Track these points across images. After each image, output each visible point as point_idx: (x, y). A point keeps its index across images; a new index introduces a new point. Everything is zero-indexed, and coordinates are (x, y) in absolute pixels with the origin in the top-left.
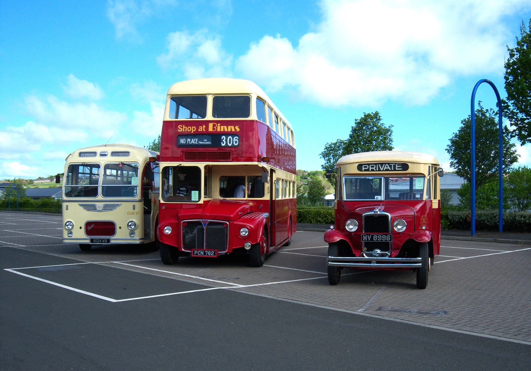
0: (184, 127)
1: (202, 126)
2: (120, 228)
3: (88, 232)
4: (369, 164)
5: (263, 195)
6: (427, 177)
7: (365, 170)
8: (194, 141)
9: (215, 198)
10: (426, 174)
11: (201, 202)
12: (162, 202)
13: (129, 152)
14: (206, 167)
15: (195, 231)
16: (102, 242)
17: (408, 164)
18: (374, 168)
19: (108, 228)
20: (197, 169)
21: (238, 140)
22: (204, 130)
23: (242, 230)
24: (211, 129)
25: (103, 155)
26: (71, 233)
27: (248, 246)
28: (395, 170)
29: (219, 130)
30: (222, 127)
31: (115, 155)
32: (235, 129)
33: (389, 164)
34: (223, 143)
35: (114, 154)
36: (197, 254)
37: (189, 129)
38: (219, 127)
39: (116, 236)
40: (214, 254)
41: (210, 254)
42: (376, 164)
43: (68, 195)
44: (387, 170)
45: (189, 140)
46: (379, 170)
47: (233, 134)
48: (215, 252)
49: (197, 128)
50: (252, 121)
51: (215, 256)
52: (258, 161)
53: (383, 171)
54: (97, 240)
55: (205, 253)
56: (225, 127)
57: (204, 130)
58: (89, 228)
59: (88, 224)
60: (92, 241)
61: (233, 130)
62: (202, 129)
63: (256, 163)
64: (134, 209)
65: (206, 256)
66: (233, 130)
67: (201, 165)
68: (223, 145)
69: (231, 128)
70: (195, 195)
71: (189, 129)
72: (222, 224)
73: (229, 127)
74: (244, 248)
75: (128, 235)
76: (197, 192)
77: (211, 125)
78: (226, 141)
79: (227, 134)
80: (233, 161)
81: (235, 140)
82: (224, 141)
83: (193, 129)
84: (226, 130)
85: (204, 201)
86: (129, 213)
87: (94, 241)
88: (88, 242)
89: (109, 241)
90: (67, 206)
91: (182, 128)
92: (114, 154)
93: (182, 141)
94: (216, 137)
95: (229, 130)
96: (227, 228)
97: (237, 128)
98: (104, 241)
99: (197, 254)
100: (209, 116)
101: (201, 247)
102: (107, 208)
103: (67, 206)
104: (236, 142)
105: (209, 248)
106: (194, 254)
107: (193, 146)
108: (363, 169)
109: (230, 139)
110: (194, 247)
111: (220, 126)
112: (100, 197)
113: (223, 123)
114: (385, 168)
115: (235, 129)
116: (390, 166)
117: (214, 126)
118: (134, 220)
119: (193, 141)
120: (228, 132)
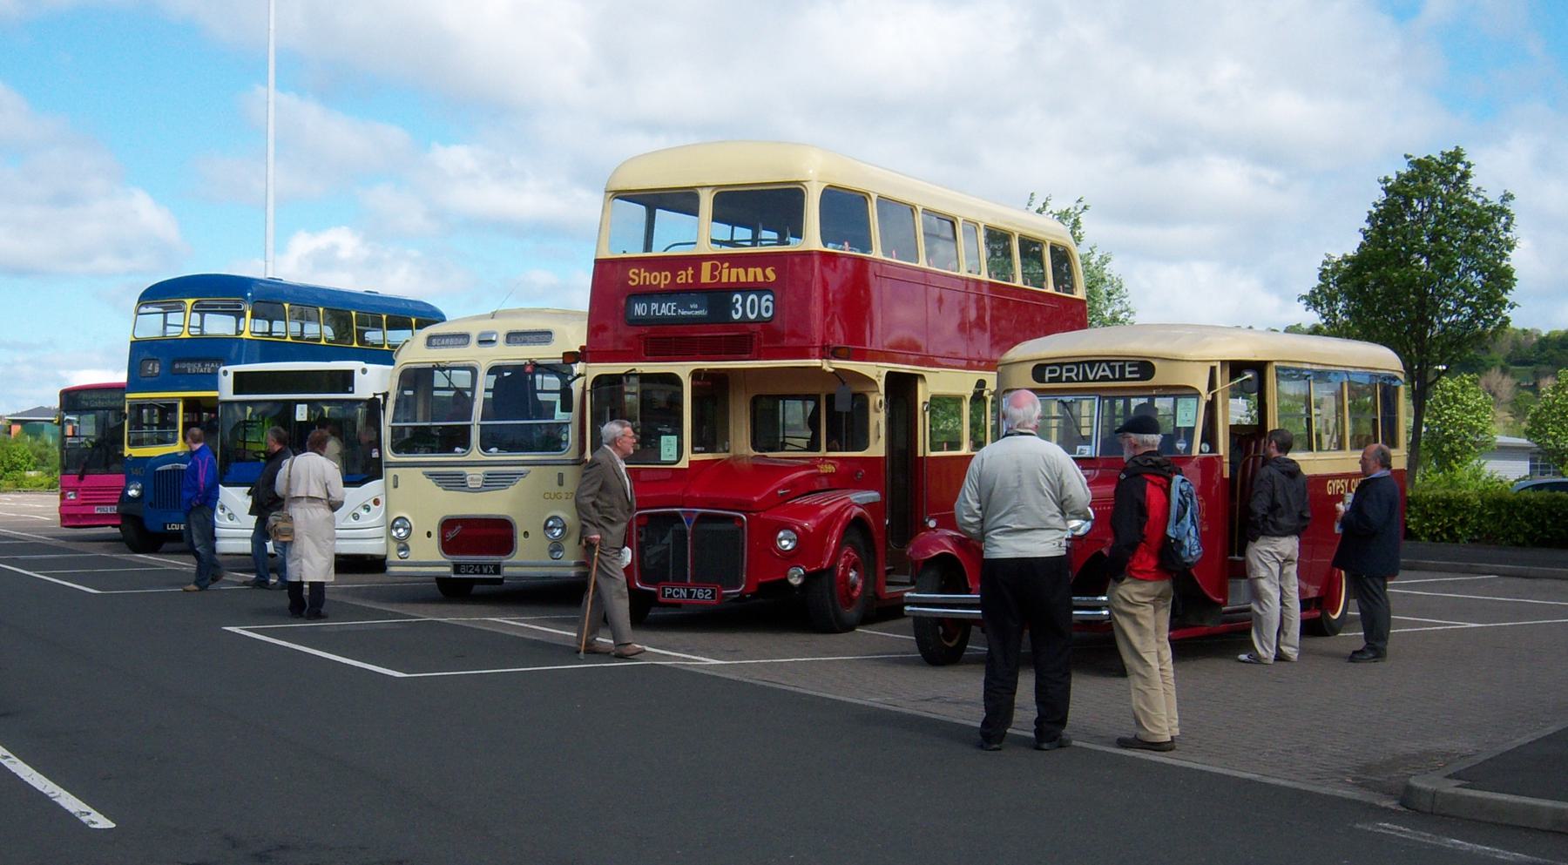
2: (526, 534)
3: (448, 547)
4: (1061, 365)
6: (1206, 396)
7: (1052, 380)
9: (738, 453)
10: (1202, 386)
11: (684, 464)
13: (549, 333)
14: (696, 375)
15: (669, 539)
17: (1155, 363)
18: (1073, 375)
19: (493, 535)
20: (673, 380)
23: (781, 534)
24: (705, 278)
25: (485, 341)
26: (406, 548)
28: (1122, 378)
29: (725, 280)
30: (734, 271)
31: (516, 342)
32: (765, 276)
33: (1108, 362)
35: (514, 337)
38: (725, 272)
39: (518, 556)
41: (703, 595)
42: (1077, 364)
43: (396, 449)
44: (1104, 379)
45: (655, 306)
46: (1086, 379)
47: (759, 288)
49: (674, 276)
50: (808, 255)
52: (822, 357)
53: (1094, 380)
54: (468, 566)
55: (690, 594)
56: (741, 271)
58: (450, 535)
59: (448, 524)
61: (760, 278)
62: (685, 277)
63: (816, 362)
64: (561, 484)
67: (683, 370)
68: (736, 317)
69: (755, 274)
70: (668, 446)
73: (751, 270)
74: (785, 582)
75: (547, 553)
76: (675, 438)
77: (706, 267)
78: (744, 305)
79: (745, 289)
81: (764, 304)
82: (738, 306)
83: (662, 279)
84: (743, 279)
86: (548, 496)
88: (447, 570)
89: (497, 568)
90: (396, 477)
92: (514, 337)
93: (639, 309)
94: (719, 296)
95: (751, 279)
97: (769, 271)
99: (670, 596)
101: (680, 580)
102: (493, 482)
103: (396, 477)
104: (767, 309)
105: (700, 581)
107: (665, 321)
108: (1047, 376)
110: (666, 579)
112: (476, 453)
114: (1100, 373)
115: (765, 276)
116: (1112, 369)
117: (714, 268)
118: (561, 515)
119: (665, 310)
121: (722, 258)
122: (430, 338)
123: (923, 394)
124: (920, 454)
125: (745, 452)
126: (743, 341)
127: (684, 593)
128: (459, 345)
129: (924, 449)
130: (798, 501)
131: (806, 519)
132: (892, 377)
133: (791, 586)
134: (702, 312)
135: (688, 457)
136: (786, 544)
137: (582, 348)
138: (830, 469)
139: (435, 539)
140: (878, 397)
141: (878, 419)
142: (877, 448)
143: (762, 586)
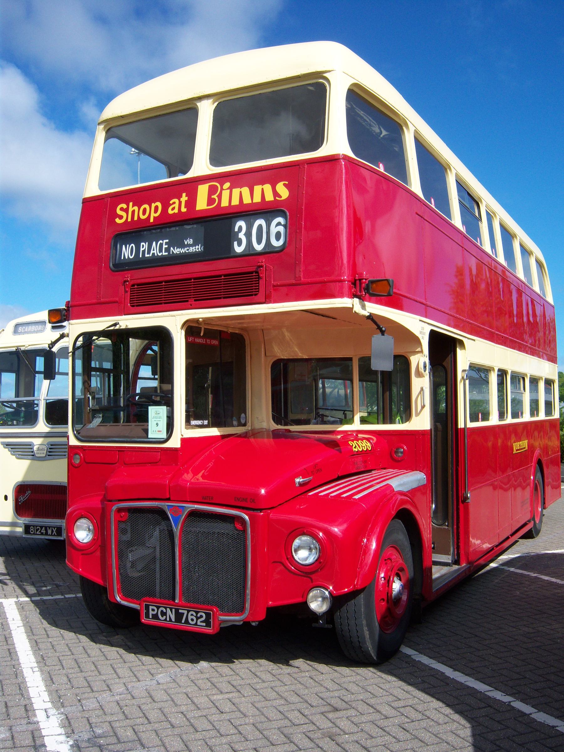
1: (179, 197)
3: (19, 509)
5: (407, 416)
8: (157, 249)
9: (257, 426)
11: (175, 443)
12: (73, 442)
14: (191, 329)
16: (46, 534)
20: (160, 336)
21: (285, 226)
22: (184, 210)
23: (297, 542)
24: (202, 204)
30: (236, 192)
34: (240, 244)
37: (145, 210)
38: (225, 195)
40: (207, 622)
41: (195, 621)
47: (267, 210)
48: (208, 615)
49: (166, 206)
51: (209, 630)
55: (179, 616)
58: (22, 499)
60: (27, 528)
61: (269, 197)
62: (177, 206)
65: (182, 626)
66: (269, 197)
67: (174, 321)
69: (264, 192)
73: (258, 189)
74: (305, 605)
76: (163, 410)
77: (203, 190)
78: (248, 235)
80: (267, 300)
81: (274, 230)
82: (242, 236)
83: (151, 212)
84: (247, 200)
87: (32, 529)
91: (126, 211)
93: (127, 252)
94: (218, 224)
95: (257, 199)
96: (245, 530)
98: (50, 532)
99: (155, 617)
100: (201, 165)
106: (147, 615)
107: (156, 262)
109: (260, 227)
111: (231, 188)
117: (213, 190)
119: (155, 251)
120: (253, 204)
121: (221, 178)
122: (17, 326)
123: (464, 359)
124: (461, 425)
125: (264, 425)
126: (245, 282)
128: (37, 332)
129: (464, 421)
130: (323, 491)
131: (333, 522)
132: (434, 336)
134: (198, 248)
135: (182, 431)
136: (304, 554)
137: (68, 303)
138: (364, 446)
139: (10, 503)
140: (420, 360)
141: (421, 385)
142: (421, 421)
143: (271, 611)
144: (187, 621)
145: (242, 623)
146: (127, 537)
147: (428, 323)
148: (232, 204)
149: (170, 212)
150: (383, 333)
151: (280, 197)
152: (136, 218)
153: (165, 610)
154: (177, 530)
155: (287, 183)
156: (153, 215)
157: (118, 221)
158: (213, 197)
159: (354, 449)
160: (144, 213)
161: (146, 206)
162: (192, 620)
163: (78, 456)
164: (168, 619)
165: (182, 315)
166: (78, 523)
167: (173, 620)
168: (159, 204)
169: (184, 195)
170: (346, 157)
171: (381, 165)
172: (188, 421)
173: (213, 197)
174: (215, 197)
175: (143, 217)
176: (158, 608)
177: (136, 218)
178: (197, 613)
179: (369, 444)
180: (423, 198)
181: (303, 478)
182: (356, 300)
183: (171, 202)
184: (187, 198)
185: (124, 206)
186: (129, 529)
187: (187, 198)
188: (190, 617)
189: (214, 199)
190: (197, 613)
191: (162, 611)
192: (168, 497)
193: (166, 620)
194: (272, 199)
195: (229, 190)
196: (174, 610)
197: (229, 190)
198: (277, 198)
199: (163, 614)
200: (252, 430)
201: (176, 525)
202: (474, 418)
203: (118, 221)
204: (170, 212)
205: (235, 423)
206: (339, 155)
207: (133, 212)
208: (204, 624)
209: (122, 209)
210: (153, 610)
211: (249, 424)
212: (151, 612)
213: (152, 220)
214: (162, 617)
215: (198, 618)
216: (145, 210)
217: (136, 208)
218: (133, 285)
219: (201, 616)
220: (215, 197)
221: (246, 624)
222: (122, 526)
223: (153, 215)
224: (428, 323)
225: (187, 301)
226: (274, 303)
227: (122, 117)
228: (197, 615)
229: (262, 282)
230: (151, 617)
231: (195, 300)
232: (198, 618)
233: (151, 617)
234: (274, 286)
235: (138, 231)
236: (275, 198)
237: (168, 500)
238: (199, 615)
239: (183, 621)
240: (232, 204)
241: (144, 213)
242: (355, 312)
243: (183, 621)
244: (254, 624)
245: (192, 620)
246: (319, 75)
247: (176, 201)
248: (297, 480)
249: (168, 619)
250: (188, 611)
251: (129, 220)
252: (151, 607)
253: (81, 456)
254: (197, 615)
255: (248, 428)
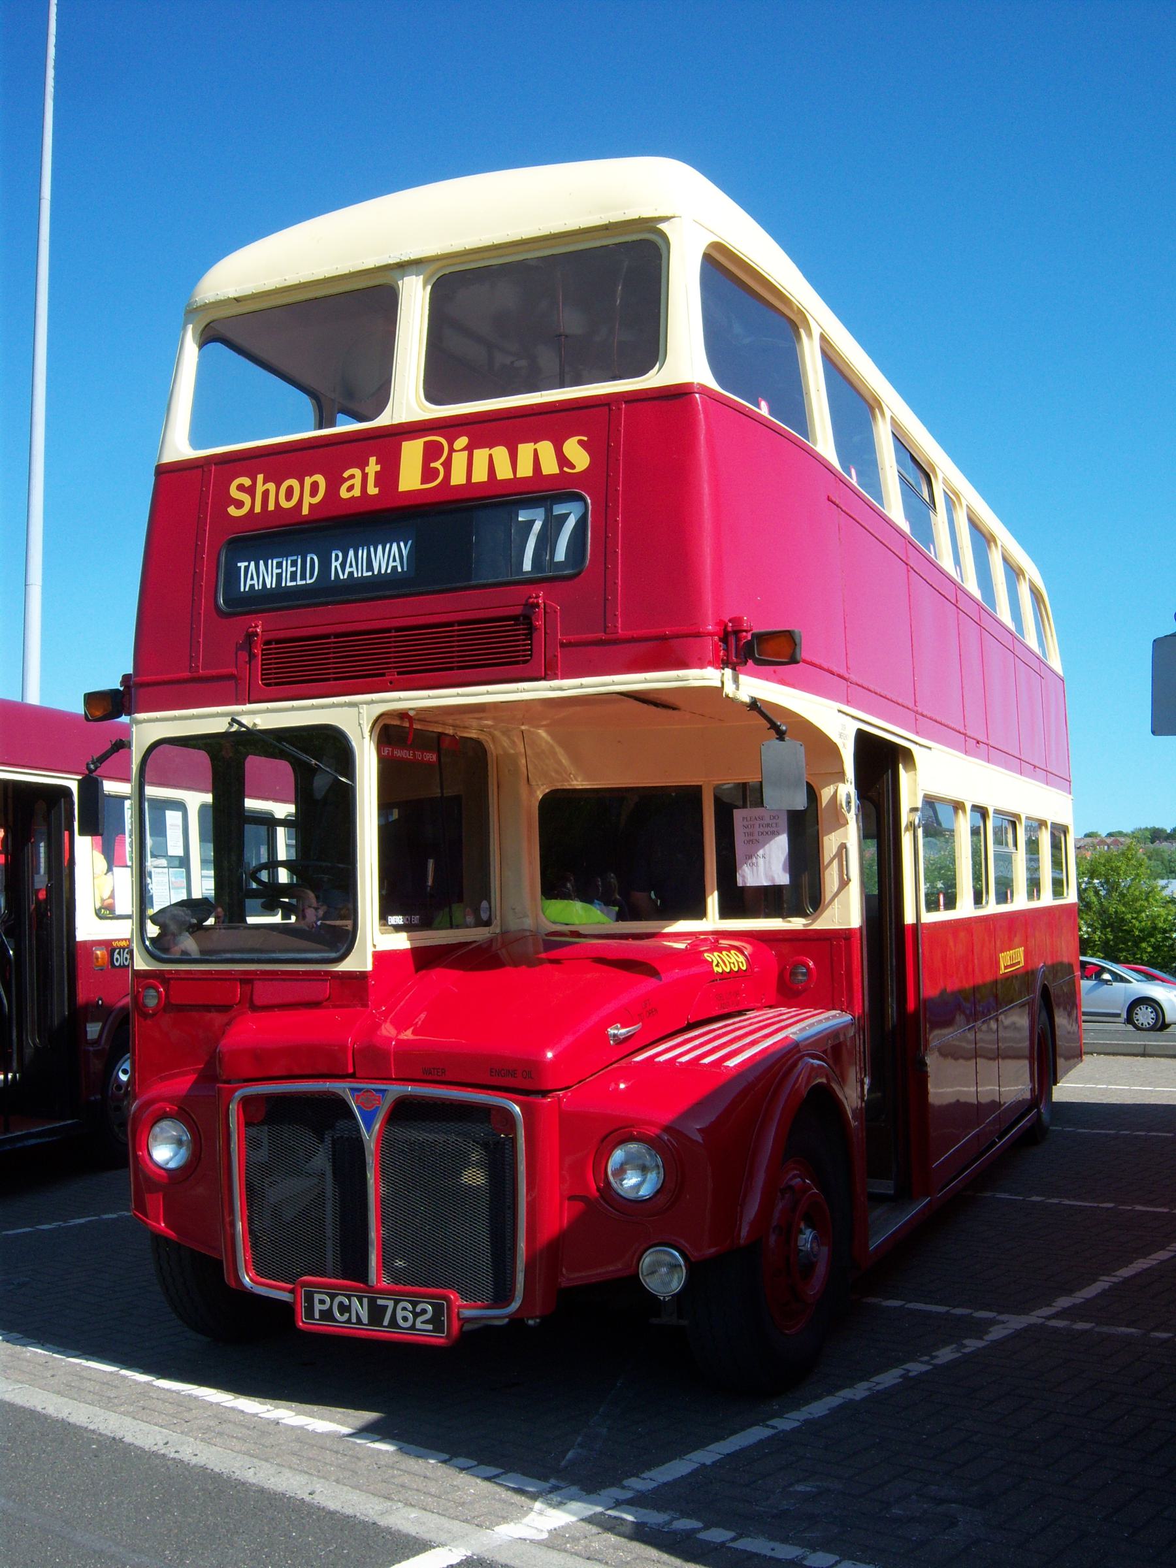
0: (260, 489)
1: (362, 465)
9: (513, 925)
14: (389, 732)
22: (372, 490)
23: (618, 1155)
27: (663, 1273)
32: (563, 460)
36: (327, 1315)
37: (289, 494)
38: (459, 461)
40: (436, 1321)
48: (438, 1309)
49: (334, 483)
50: (679, 395)
51: (440, 1339)
52: (722, 663)
55: (376, 1313)
56: (500, 453)
57: (372, 490)
61: (550, 467)
62: (359, 482)
65: (382, 1332)
66: (550, 467)
67: (355, 716)
69: (537, 457)
71: (289, 494)
72: (485, 1112)
73: (525, 451)
74: (633, 1281)
77: (412, 453)
83: (304, 494)
84: (504, 472)
85: (379, 957)
91: (251, 490)
95: (525, 470)
99: (327, 1315)
100: (408, 401)
111: (470, 449)
113: (484, 431)
115: (563, 460)
117: (432, 452)
123: (911, 790)
124: (909, 918)
127: (360, 1309)
130: (664, 1052)
132: (866, 744)
133: (651, 1298)
137: (126, 679)
141: (846, 840)
142: (845, 910)
144: (393, 1322)
145: (507, 1320)
146: (262, 1155)
147: (853, 717)
148: (474, 480)
149: (344, 494)
150: (781, 736)
151: (573, 467)
152: (271, 507)
153: (346, 1302)
154: (370, 1139)
155: (585, 439)
156: (308, 500)
157: (233, 511)
158: (432, 465)
159: (716, 969)
160: (289, 496)
161: (294, 482)
162: (405, 1319)
163: (152, 992)
164: (354, 1320)
165: (372, 702)
166: (156, 1129)
167: (365, 1320)
168: (320, 479)
169: (373, 460)
170: (704, 390)
171: (763, 404)
172: (383, 916)
173: (432, 465)
174: (437, 465)
175: (285, 505)
176: (333, 1297)
177: (271, 507)
178: (414, 1304)
179: (742, 959)
180: (840, 469)
181: (623, 1027)
182: (728, 672)
183: (346, 475)
184: (378, 468)
185: (247, 482)
186: (265, 1141)
187: (378, 468)
188: (400, 1314)
189: (437, 471)
190: (414, 1304)
191: (341, 1304)
192: (351, 1071)
193: (349, 1321)
194: (557, 471)
195: (466, 453)
196: (365, 1301)
197: (466, 453)
198: (566, 469)
199: (344, 1309)
200: (504, 933)
201: (369, 1128)
202: (932, 905)
203: (233, 511)
204: (344, 494)
205: (470, 919)
206: (692, 384)
207: (266, 494)
208: (430, 1327)
209: (241, 488)
210: (322, 1302)
211: (496, 922)
212: (318, 1307)
213: (305, 511)
214: (342, 1314)
215: (416, 1315)
216: (290, 490)
217: (271, 486)
218: (268, 643)
219: (424, 1311)
220: (437, 465)
221: (516, 1321)
222: (253, 1131)
223: (308, 500)
224: (853, 717)
225: (383, 675)
226: (562, 678)
227: (237, 300)
228: (414, 1308)
229: (539, 636)
230: (317, 1316)
231: (399, 673)
232: (416, 1315)
233: (317, 1316)
234: (562, 645)
235: (277, 534)
236: (561, 468)
237: (353, 1076)
238: (418, 1309)
239: (386, 1323)
240: (474, 480)
241: (289, 496)
242: (727, 696)
243: (386, 1323)
244: (531, 1322)
245: (405, 1319)
246: (650, 225)
247: (357, 472)
248: (611, 1031)
249: (354, 1320)
250: (397, 1302)
251: (258, 509)
252: (317, 1297)
253: (158, 992)
254: (414, 1308)
255: (495, 929)
